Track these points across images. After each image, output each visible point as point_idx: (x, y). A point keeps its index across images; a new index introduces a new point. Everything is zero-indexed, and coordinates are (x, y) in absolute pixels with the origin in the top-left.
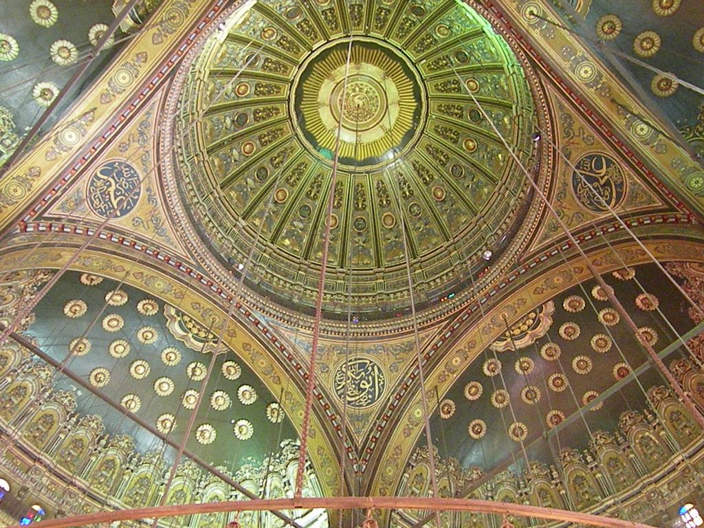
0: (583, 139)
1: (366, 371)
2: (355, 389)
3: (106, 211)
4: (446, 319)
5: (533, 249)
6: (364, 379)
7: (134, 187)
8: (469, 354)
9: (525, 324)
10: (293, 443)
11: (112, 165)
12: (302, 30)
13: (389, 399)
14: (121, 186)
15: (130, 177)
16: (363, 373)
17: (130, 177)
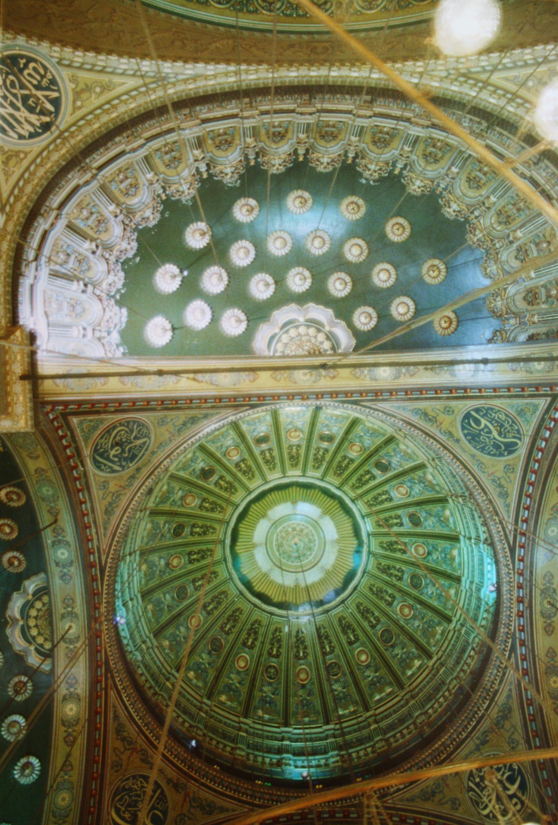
0: (185, 815)
1: (126, 459)
2: (121, 440)
3: (487, 412)
4: (106, 562)
5: (112, 694)
6: (121, 453)
7: (473, 439)
8: (58, 569)
9: (36, 626)
10: (118, 327)
11: (510, 453)
12: (394, 567)
13: (83, 466)
14: (489, 437)
15: (484, 447)
16: (126, 455)
17: (484, 447)
